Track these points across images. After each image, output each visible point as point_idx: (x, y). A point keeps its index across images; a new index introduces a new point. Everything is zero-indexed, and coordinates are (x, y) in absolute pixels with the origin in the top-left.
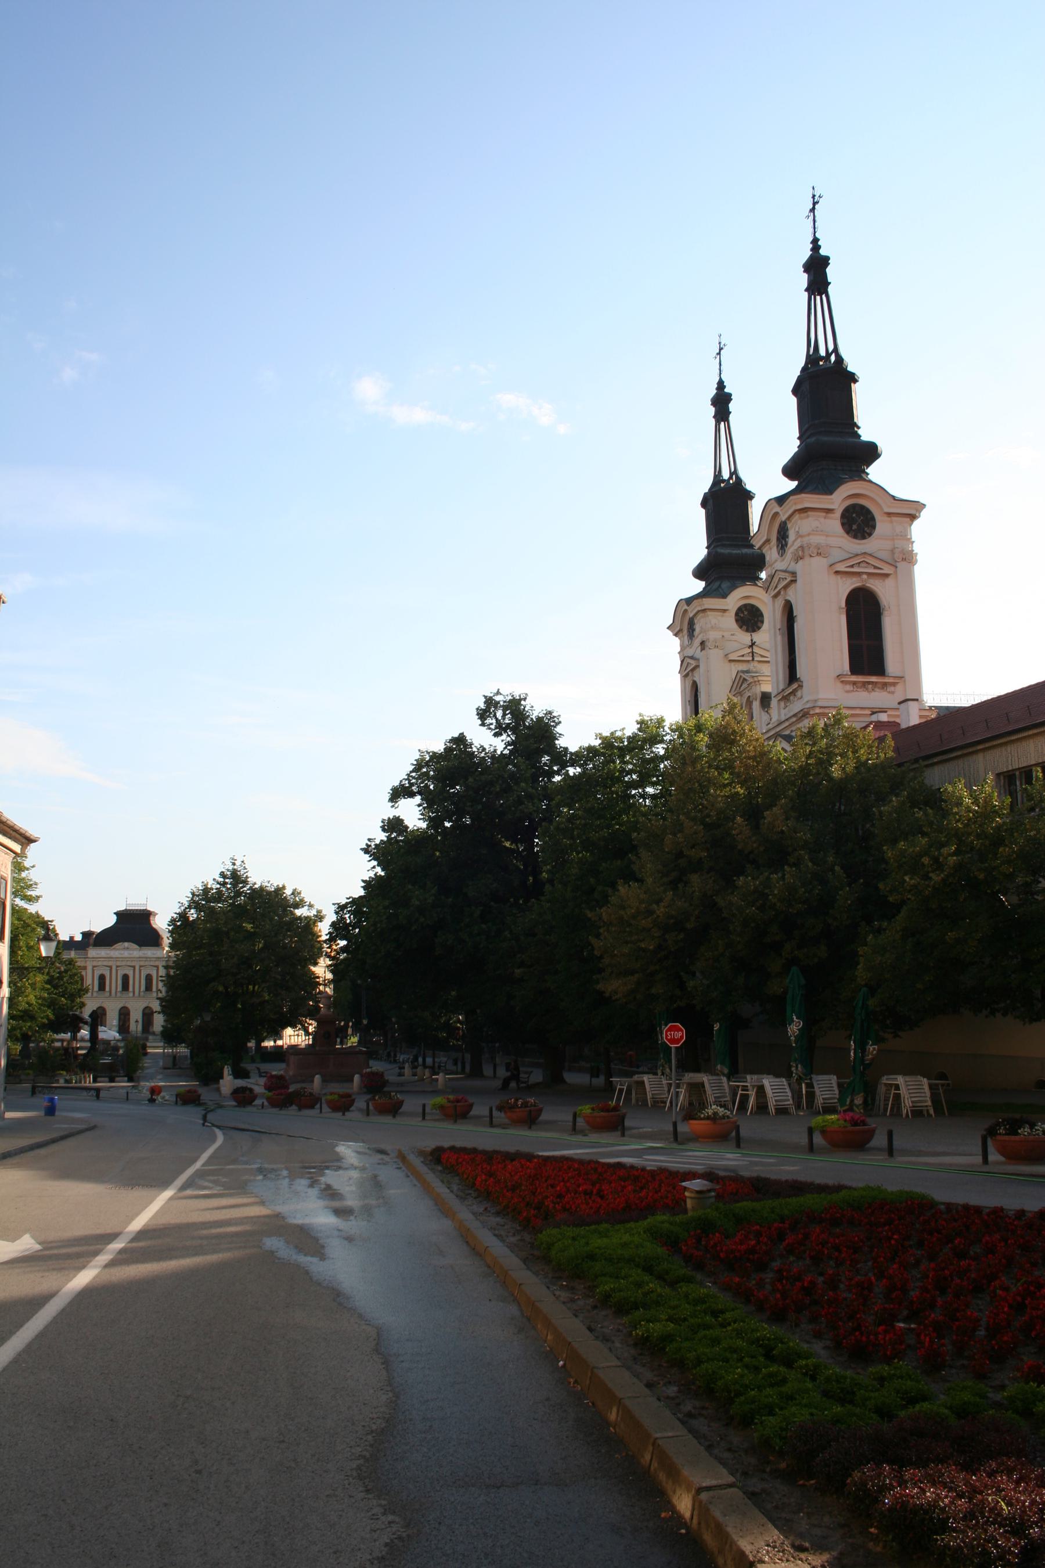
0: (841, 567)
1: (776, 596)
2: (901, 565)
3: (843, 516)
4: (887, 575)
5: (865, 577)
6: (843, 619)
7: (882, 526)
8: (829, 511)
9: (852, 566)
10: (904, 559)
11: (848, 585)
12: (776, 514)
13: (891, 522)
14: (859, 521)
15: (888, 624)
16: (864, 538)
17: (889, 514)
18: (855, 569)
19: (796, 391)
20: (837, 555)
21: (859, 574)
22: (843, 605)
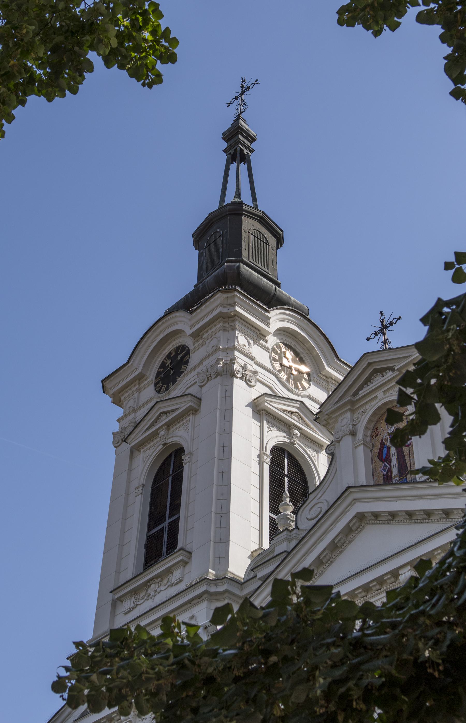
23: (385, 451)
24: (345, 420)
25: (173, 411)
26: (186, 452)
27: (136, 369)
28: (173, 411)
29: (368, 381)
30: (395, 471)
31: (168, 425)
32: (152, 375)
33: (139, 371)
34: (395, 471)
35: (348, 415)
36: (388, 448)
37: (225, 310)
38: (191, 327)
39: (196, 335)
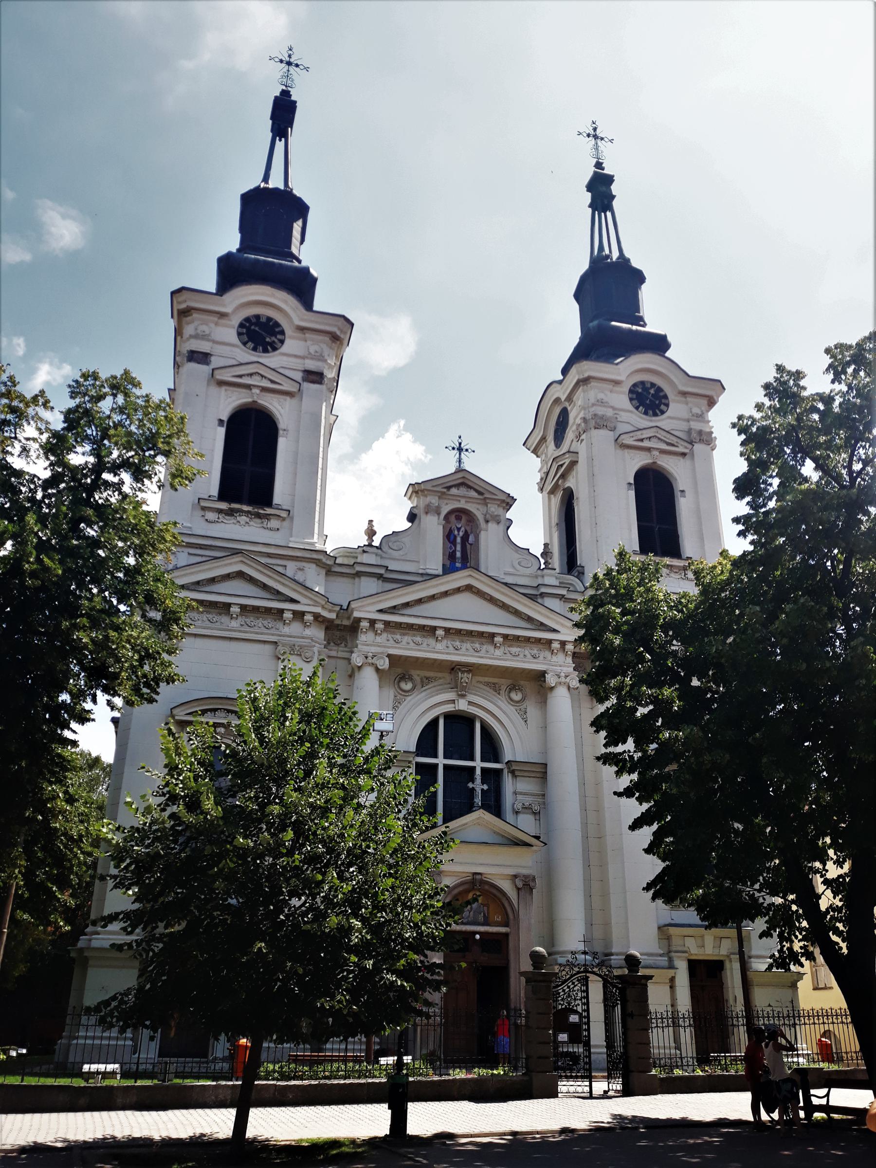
0: (628, 440)
1: (552, 492)
2: (698, 447)
3: (631, 391)
4: (684, 455)
5: (656, 453)
6: (632, 493)
7: (676, 409)
8: (617, 383)
9: (642, 440)
10: (701, 441)
11: (637, 462)
12: (557, 401)
13: (687, 404)
14: (649, 399)
15: (684, 507)
16: (655, 415)
17: (684, 394)
18: (646, 444)
19: (578, 296)
20: (622, 428)
21: (649, 449)
22: (632, 482)
23: (452, 537)
24: (434, 500)
25: (272, 382)
26: (281, 425)
27: (224, 306)
28: (272, 382)
29: (458, 486)
30: (458, 554)
31: (264, 389)
32: (236, 321)
33: (228, 310)
34: (458, 554)
35: (437, 498)
36: (455, 537)
37: (338, 333)
38: (302, 320)
39: (302, 329)
